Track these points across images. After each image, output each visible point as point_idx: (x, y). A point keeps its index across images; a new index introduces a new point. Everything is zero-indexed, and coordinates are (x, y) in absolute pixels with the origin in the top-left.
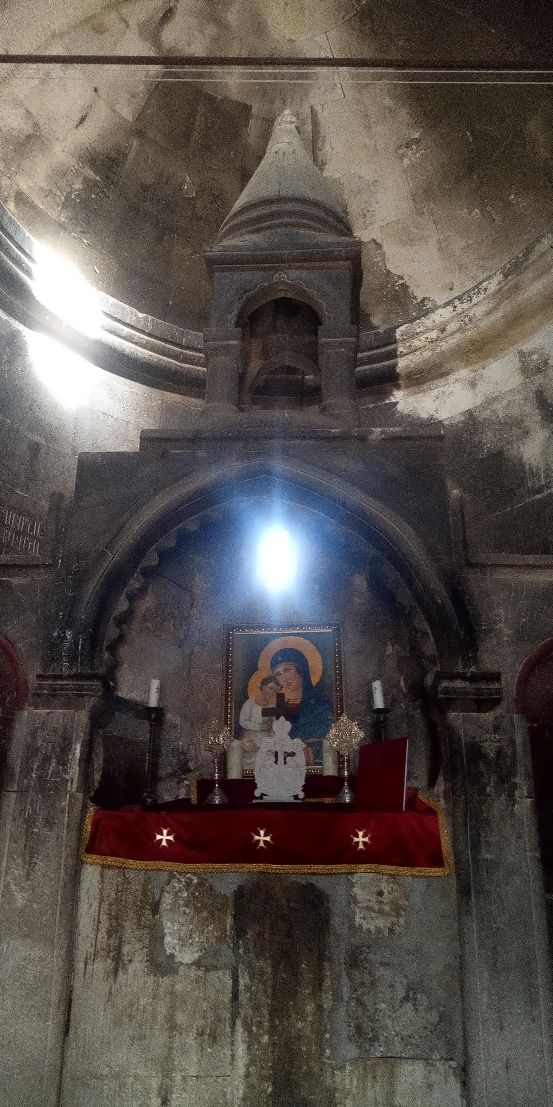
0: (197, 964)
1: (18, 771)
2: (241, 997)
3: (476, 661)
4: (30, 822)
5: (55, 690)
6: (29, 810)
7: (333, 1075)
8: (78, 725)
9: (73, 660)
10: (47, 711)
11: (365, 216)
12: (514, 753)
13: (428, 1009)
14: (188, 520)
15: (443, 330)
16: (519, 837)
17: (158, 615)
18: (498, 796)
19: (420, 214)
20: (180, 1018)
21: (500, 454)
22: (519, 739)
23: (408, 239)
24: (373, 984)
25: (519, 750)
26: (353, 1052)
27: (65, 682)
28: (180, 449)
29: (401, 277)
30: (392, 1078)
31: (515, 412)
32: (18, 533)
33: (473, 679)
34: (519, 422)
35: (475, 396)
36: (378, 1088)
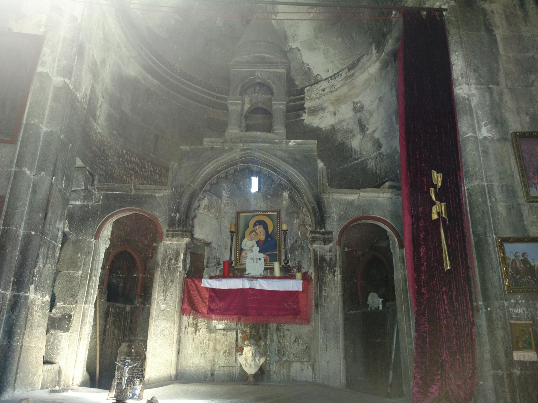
0: (224, 329)
1: (160, 263)
2: (239, 340)
3: (324, 227)
4: (165, 281)
6: (165, 277)
7: (270, 366)
10: (170, 242)
11: (294, 37)
12: (336, 259)
13: (302, 345)
15: (323, 90)
16: (336, 288)
18: (329, 274)
19: (317, 38)
20: (218, 347)
21: (343, 144)
22: (338, 255)
23: (312, 48)
24: (284, 336)
25: (338, 258)
26: (277, 358)
29: (308, 65)
30: (290, 366)
31: (350, 127)
32: (151, 172)
33: (323, 233)
34: (351, 131)
35: (335, 119)
36: (284, 370)
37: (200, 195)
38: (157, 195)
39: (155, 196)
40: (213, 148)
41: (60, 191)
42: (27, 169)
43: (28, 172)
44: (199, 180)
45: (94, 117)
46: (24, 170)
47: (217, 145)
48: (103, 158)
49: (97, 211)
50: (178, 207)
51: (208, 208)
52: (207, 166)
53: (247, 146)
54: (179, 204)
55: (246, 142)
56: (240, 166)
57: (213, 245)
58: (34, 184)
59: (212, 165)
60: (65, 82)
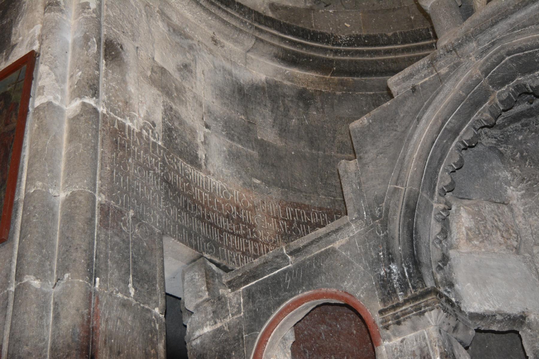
5: (398, 317)
8: (431, 342)
9: (404, 287)
10: (400, 339)
14: (461, 133)
17: (481, 231)
27: (404, 308)
28: (425, 77)
37: (435, 206)
38: (337, 245)
39: (334, 250)
40: (414, 89)
41: (125, 305)
42: (32, 277)
43: (36, 283)
44: (412, 168)
45: (194, 161)
46: (25, 280)
47: (422, 78)
48: (242, 232)
49: (240, 332)
50: (388, 249)
51: (480, 233)
52: (418, 131)
53: (485, 39)
54: (388, 240)
55: (482, 31)
56: (499, 95)
57: (532, 317)
58: (55, 304)
59: (427, 123)
60: (84, 104)
